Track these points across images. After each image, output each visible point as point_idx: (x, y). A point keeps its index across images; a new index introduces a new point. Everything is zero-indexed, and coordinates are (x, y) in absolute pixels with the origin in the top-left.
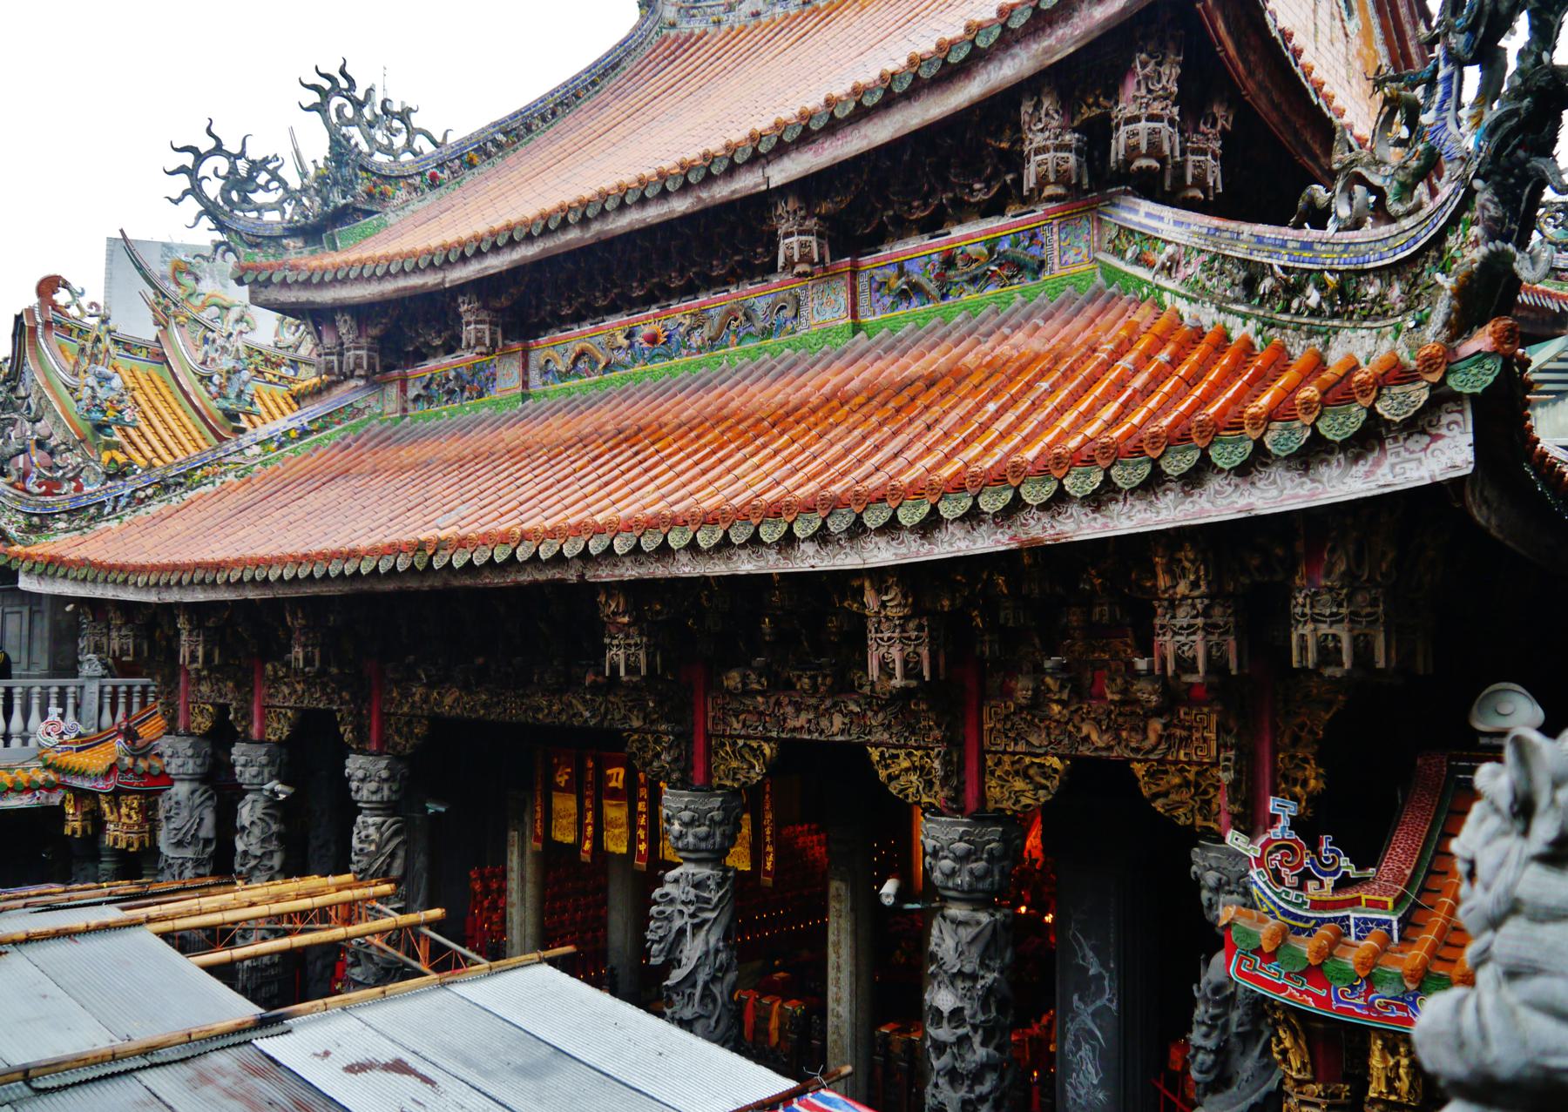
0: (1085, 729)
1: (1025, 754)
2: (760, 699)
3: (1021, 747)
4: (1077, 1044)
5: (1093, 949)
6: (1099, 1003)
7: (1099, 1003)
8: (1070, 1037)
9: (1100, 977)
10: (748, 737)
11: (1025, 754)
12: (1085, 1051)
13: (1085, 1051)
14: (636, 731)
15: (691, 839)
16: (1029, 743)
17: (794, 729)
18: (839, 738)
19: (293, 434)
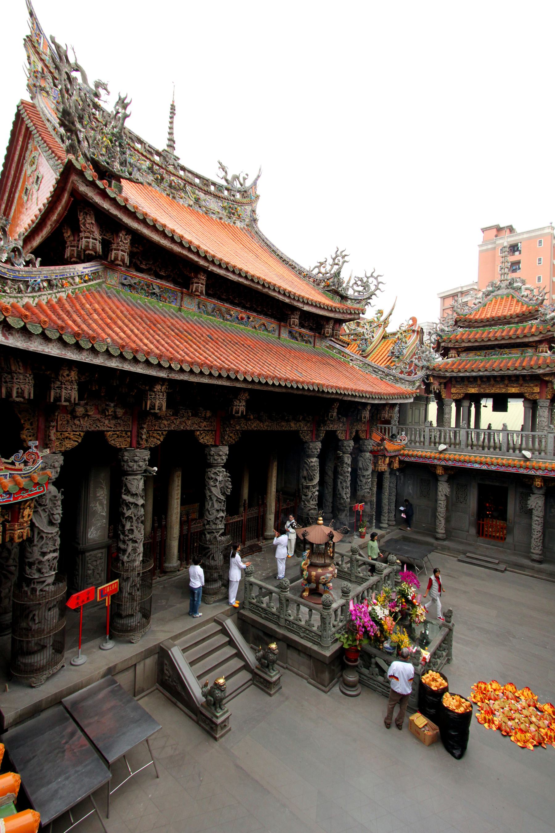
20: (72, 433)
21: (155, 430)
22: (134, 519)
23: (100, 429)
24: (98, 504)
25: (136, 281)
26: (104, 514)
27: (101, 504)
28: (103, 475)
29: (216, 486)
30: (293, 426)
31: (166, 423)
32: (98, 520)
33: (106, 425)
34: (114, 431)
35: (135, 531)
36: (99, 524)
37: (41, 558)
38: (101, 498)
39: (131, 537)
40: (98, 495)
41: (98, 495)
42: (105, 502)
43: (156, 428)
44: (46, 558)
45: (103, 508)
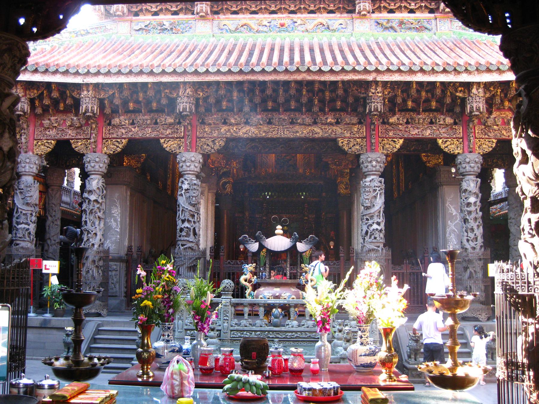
0: (503, 132)
1: (487, 138)
2: (400, 126)
3: (486, 136)
4: (450, 234)
5: (454, 208)
6: (456, 222)
7: (456, 222)
8: (448, 233)
9: (456, 215)
10: (394, 138)
11: (487, 138)
12: (453, 236)
13: (453, 236)
14: (345, 138)
15: (378, 167)
16: (489, 136)
17: (412, 135)
18: (430, 136)
19: (83, 32)
20: (45, 141)
21: (114, 138)
22: (88, 212)
23: (66, 137)
24: (112, 220)
25: (148, 22)
26: (118, 230)
27: (116, 221)
28: (117, 195)
29: (181, 195)
30: (319, 132)
31: (124, 131)
32: (113, 235)
33: (70, 134)
34: (77, 139)
35: (88, 222)
36: (114, 239)
37: (16, 225)
38: (115, 215)
39: (85, 227)
40: (113, 212)
41: (113, 212)
42: (119, 220)
43: (115, 136)
44: (20, 226)
45: (117, 225)
